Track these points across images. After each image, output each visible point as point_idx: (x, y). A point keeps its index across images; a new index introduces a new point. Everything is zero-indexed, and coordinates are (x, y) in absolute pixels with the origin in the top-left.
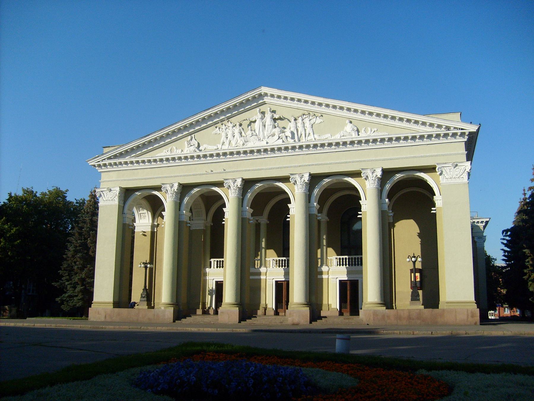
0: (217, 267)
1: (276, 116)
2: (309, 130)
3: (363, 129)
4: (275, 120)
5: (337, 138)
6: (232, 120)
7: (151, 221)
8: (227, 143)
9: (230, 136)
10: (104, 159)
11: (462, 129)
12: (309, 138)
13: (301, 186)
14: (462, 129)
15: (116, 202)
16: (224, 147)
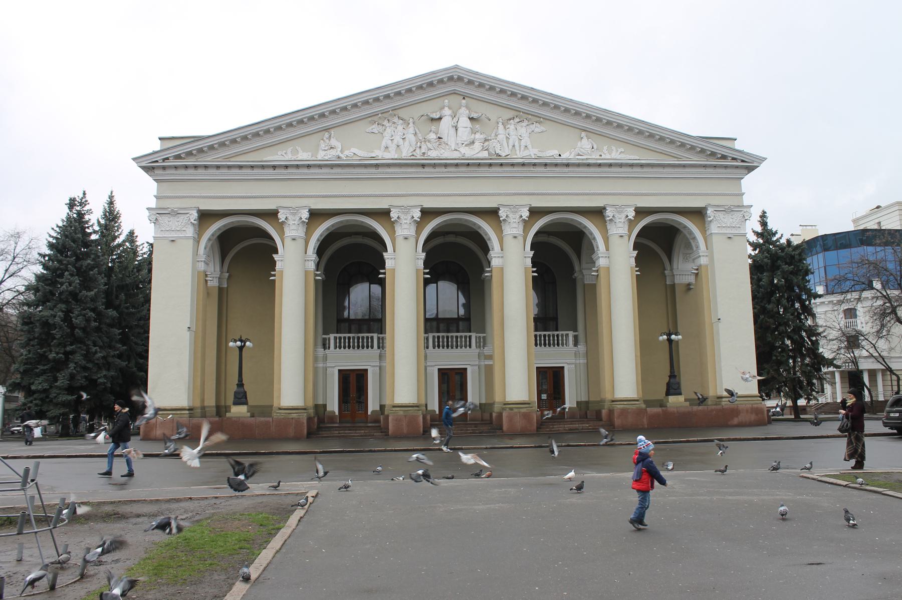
0: (336, 348)
1: (475, 115)
2: (526, 141)
3: (605, 148)
4: (471, 119)
5: (568, 156)
6: (401, 113)
7: (218, 268)
8: (393, 148)
9: (398, 139)
10: (167, 159)
11: (743, 161)
12: (525, 153)
13: (515, 225)
14: (743, 161)
15: (190, 232)
16: (387, 155)
